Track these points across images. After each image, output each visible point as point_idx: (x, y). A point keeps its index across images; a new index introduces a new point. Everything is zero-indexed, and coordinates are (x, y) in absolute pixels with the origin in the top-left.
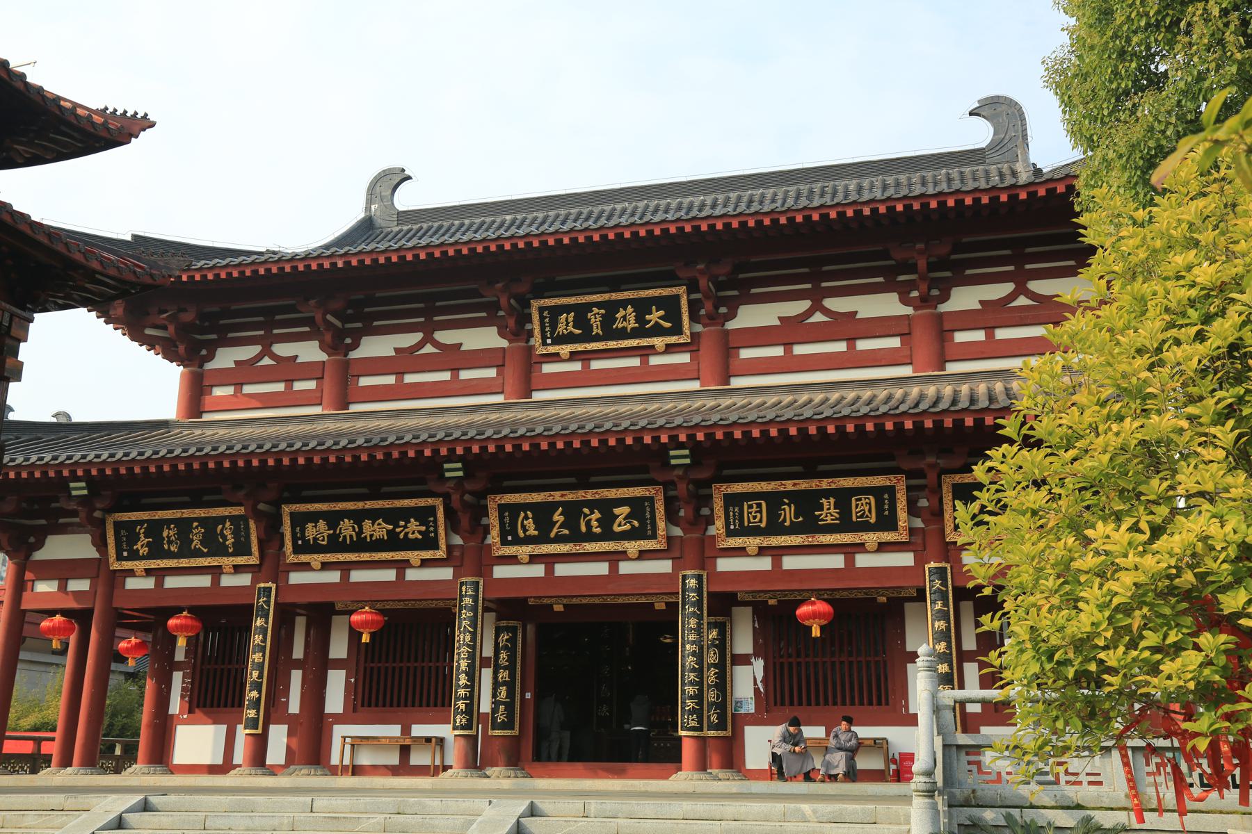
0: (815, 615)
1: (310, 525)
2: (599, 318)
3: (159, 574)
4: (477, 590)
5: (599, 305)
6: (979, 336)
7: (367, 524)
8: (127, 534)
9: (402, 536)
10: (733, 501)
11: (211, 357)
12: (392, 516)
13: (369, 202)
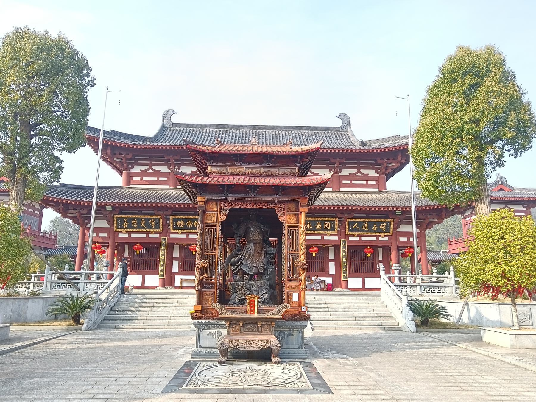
0: (314, 251)
3: (130, 233)
6: (348, 182)
11: (132, 168)
13: (163, 119)
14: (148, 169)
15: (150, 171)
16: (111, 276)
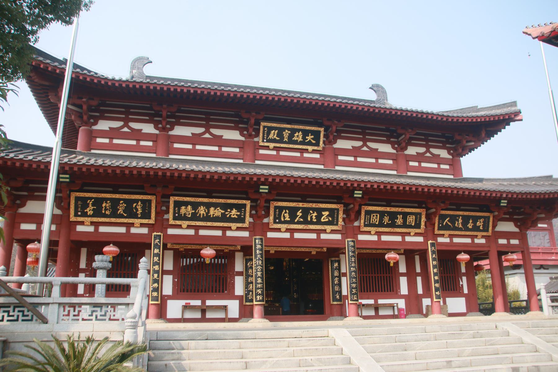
1: (183, 207)
2: (288, 135)
3: (96, 225)
4: (262, 242)
5: (289, 129)
6: (416, 164)
8: (82, 203)
9: (228, 216)
10: (368, 213)
11: (96, 123)
12: (225, 207)
14: (122, 127)
15: (126, 129)
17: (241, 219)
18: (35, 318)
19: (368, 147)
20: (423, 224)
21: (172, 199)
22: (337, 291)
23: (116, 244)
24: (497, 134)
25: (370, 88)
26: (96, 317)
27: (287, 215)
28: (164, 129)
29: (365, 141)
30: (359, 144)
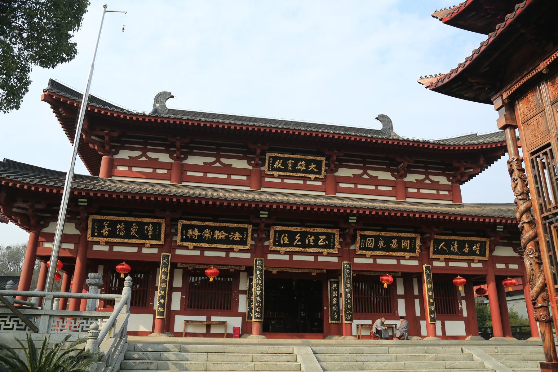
0: (388, 280)
2: (291, 164)
3: (111, 245)
5: (292, 159)
6: (415, 190)
7: (217, 232)
9: (231, 239)
10: (363, 237)
11: (117, 153)
12: (228, 230)
14: (141, 156)
16: (110, 303)
17: (243, 242)
18: (28, 328)
19: (368, 175)
20: (418, 248)
21: (180, 222)
22: (335, 311)
23: (127, 262)
24: (497, 161)
25: (376, 119)
26: (82, 328)
27: (286, 239)
28: (178, 159)
29: (365, 169)
30: (359, 172)
